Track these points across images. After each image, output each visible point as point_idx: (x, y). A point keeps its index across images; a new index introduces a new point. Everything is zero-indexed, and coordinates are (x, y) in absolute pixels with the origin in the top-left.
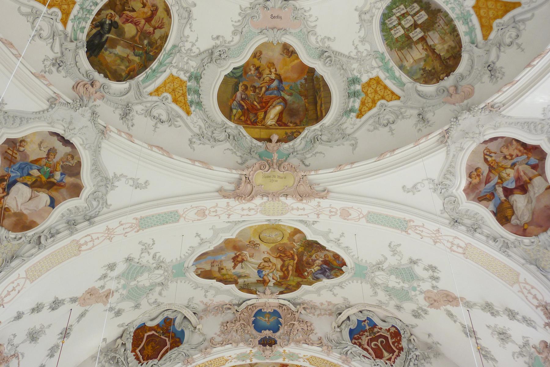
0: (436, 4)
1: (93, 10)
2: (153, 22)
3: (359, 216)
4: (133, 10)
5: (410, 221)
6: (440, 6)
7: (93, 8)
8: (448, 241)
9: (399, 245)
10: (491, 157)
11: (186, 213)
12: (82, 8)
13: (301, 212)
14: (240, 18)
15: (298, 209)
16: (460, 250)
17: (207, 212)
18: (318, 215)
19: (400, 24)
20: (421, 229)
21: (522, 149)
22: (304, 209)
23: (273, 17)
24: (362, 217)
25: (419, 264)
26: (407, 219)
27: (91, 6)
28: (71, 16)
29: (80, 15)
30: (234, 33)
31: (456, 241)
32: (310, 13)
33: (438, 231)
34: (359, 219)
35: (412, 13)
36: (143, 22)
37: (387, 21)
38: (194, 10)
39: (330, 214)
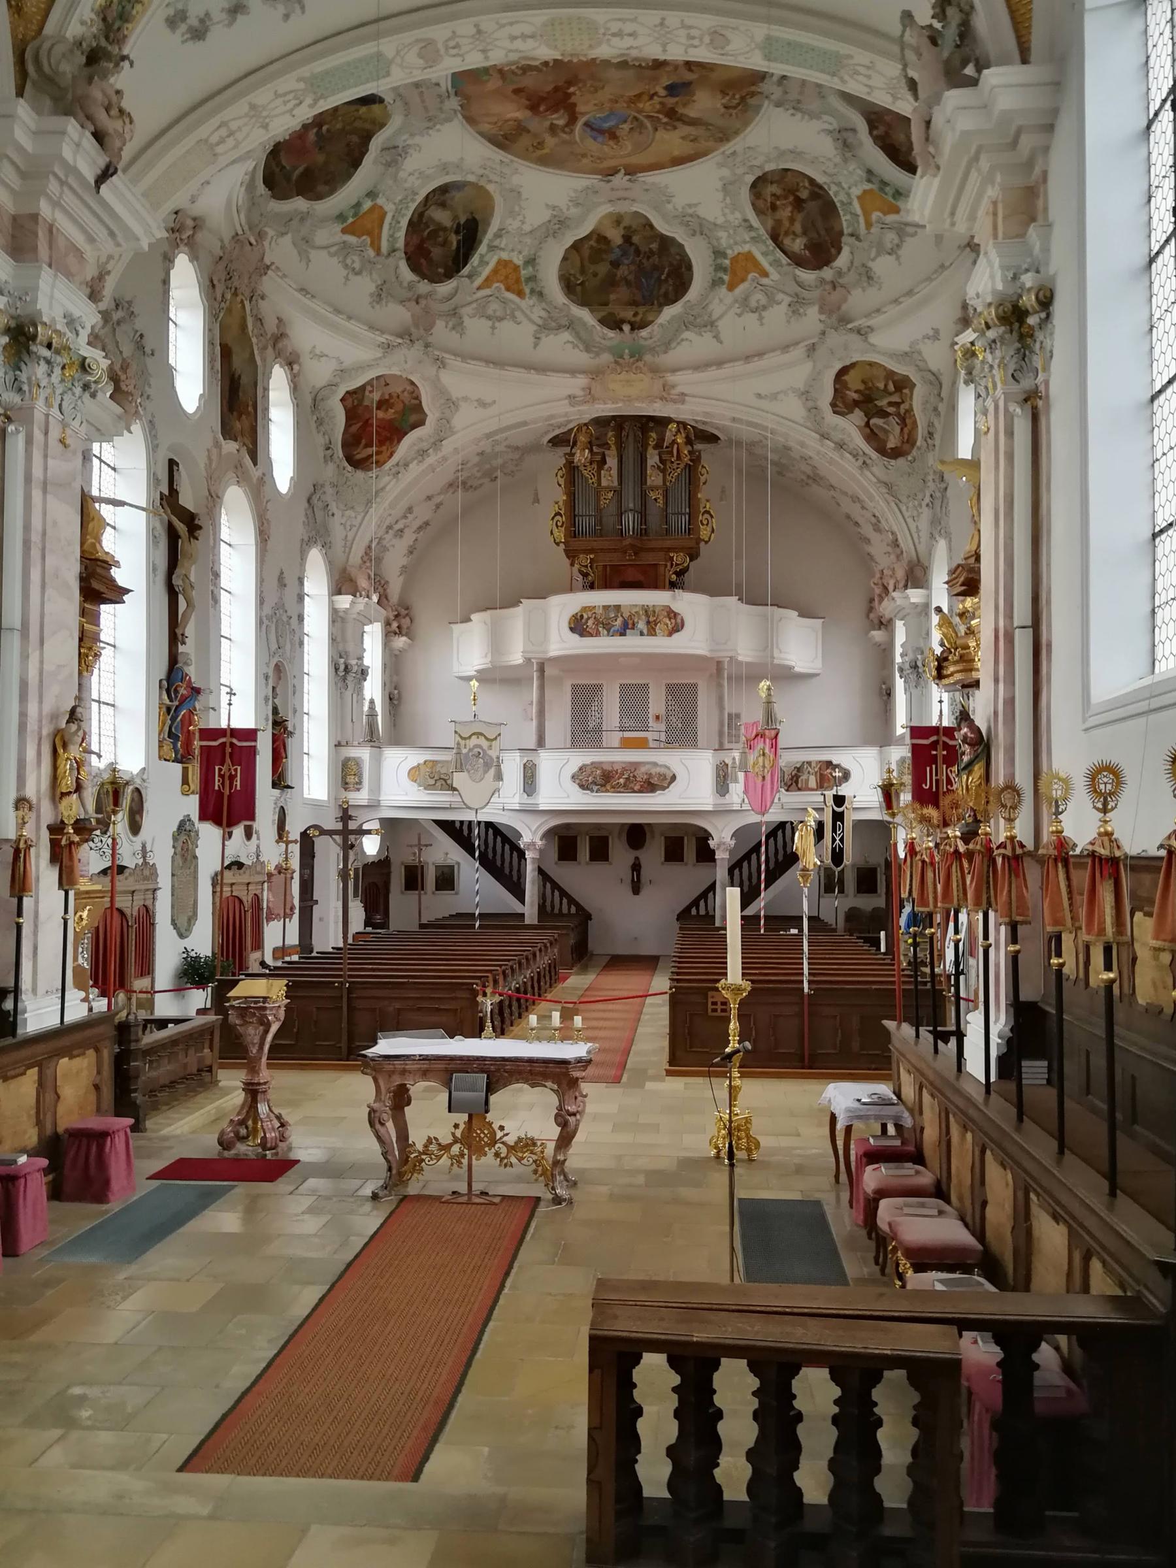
3: (402, 58)
5: (316, 101)
8: (240, 129)
9: (287, 17)
11: (748, 49)
13: (516, 30)
15: (524, 37)
16: (214, 139)
17: (707, 39)
18: (479, 32)
20: (290, 105)
22: (513, 38)
24: (394, 58)
25: (224, 16)
26: (321, 102)
31: (230, 142)
33: (265, 127)
34: (398, 52)
39: (457, 40)
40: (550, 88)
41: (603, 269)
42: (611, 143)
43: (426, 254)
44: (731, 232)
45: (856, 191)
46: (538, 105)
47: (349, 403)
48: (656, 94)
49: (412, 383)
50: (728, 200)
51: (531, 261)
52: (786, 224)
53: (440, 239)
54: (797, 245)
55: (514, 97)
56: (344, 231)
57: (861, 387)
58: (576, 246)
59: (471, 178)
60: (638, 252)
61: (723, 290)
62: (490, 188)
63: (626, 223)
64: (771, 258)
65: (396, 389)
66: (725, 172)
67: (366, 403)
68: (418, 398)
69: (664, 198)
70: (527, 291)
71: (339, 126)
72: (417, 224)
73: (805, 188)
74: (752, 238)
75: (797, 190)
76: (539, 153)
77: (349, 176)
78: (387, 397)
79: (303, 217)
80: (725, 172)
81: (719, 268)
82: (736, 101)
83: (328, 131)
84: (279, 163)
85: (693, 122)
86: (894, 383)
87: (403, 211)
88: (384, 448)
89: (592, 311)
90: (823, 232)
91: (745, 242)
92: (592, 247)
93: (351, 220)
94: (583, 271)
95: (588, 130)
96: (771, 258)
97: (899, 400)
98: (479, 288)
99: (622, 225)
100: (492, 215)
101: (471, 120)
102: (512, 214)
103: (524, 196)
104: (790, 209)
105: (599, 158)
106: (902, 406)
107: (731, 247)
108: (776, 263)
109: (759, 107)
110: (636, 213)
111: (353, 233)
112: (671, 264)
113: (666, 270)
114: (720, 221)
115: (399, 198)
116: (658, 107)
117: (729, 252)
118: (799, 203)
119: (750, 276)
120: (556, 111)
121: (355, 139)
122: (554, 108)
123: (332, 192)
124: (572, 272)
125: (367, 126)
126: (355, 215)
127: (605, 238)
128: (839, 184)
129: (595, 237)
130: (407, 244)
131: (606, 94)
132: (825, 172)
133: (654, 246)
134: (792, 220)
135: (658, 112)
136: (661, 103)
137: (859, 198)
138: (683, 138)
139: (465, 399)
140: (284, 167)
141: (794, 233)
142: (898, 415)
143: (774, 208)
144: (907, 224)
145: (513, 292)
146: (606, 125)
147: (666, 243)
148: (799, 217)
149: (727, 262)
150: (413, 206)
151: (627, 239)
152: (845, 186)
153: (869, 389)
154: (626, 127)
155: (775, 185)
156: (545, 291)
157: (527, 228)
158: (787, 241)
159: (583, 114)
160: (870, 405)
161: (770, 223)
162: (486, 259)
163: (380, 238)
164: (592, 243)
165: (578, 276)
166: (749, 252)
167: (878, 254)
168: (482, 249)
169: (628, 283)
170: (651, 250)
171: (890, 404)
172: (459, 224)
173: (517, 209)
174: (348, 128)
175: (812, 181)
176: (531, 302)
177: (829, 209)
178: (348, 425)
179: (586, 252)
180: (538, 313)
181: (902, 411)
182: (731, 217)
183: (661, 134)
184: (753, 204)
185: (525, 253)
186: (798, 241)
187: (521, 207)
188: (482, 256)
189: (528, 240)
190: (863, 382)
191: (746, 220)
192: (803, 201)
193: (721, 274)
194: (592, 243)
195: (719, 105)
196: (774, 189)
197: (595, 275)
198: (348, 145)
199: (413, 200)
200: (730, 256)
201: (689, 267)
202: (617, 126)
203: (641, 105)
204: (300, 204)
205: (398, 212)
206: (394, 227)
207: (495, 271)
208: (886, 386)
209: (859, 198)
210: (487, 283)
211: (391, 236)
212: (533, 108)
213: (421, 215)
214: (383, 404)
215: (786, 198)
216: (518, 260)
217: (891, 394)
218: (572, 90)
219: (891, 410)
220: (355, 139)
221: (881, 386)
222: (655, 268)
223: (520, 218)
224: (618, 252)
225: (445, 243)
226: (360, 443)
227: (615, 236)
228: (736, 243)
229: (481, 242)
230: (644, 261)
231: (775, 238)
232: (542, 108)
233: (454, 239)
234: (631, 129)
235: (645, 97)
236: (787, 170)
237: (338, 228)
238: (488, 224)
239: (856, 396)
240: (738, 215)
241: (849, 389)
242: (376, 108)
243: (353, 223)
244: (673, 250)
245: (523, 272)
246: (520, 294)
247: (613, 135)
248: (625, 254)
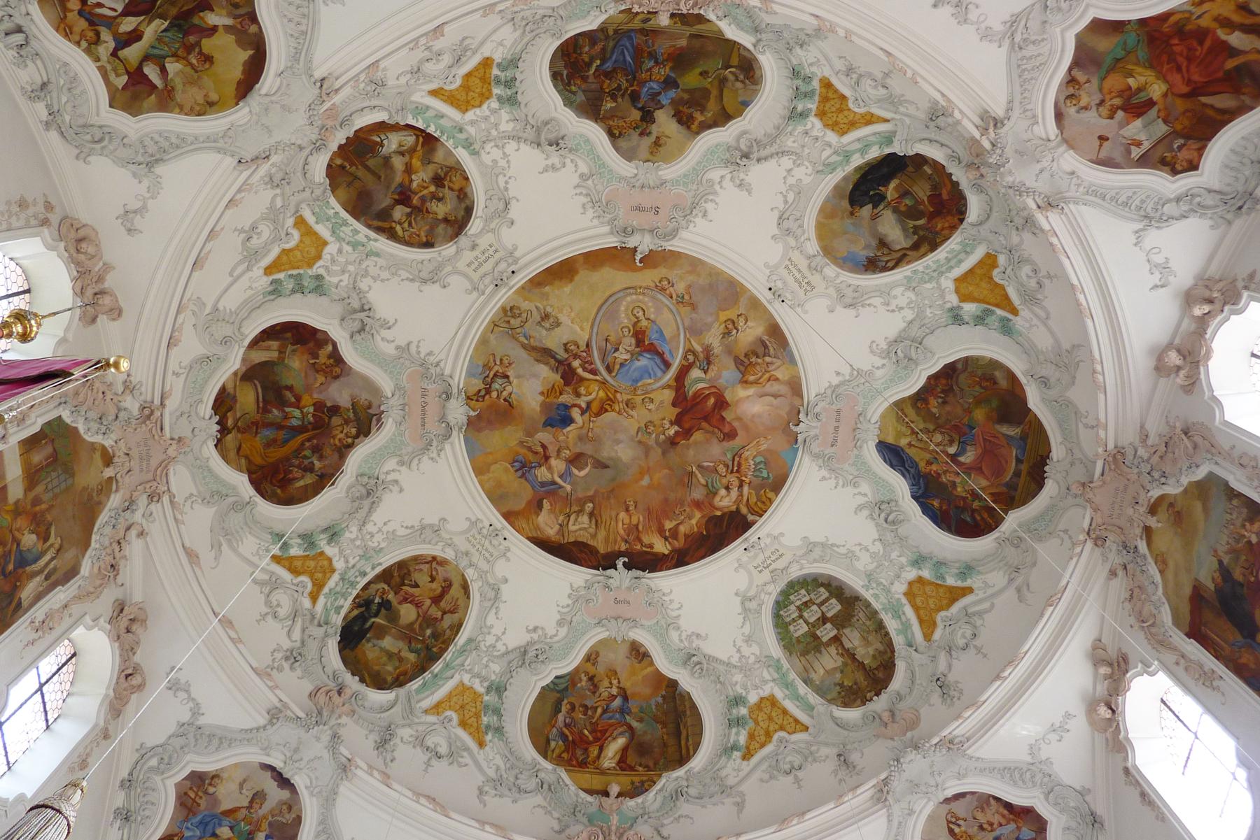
0: (851, 588)
1: (358, 583)
2: (443, 604)
4: (417, 586)
6: (857, 591)
7: (359, 579)
10: (959, 826)
12: (343, 579)
14: (570, 602)
19: (801, 617)
21: (1006, 812)
23: (617, 602)
27: (356, 577)
28: (326, 590)
29: (338, 589)
30: (560, 623)
32: (671, 597)
35: (818, 601)
36: (428, 602)
37: (781, 613)
38: (503, 587)
40: (697, 436)
41: (691, 79)
42: (644, 323)
43: (935, 198)
44: (494, 133)
45: (331, 249)
46: (715, 404)
47: (1184, 155)
48: (583, 412)
49: (1059, 116)
50: (501, 180)
51: (795, 115)
52: (416, 163)
53: (908, 202)
54: (392, 142)
55: (736, 424)
56: (1015, 312)
57: (207, 45)
58: (724, 117)
59: (831, 270)
60: (635, 97)
61: (498, 57)
62: (813, 247)
63: (647, 142)
64: (430, 114)
65: (1095, 121)
66: (508, 236)
67: (1161, 129)
68: (1071, 81)
69: (590, 182)
70: (816, 84)
71: (938, 437)
72: (927, 241)
73: (400, 223)
74: (461, 130)
75: (409, 215)
76: (731, 314)
77: (966, 360)
78: (1120, 114)
79: (1044, 382)
80: (508, 236)
81: (509, 83)
82: (496, 386)
83: (951, 442)
84: (1017, 474)
85: (544, 354)
86: (155, 87)
87: (934, 267)
88: (1205, 22)
89: (720, 32)
90: (361, 172)
91: (472, 123)
92: (703, 109)
93: (999, 312)
94: (723, 82)
95: (667, 356)
96: (430, 114)
97: (120, 53)
98: (887, 121)
99: (653, 138)
100: (826, 201)
101: (796, 388)
102: (798, 189)
103: (776, 214)
104: (415, 185)
105: (664, 290)
106: (112, 45)
107: (494, 111)
108: (420, 110)
109: (470, 374)
110: (629, 159)
111: (1006, 297)
112: (584, 79)
113: (592, 72)
114: (511, 146)
115: (929, 286)
116: (582, 390)
117: (494, 104)
118: (404, 197)
119: (458, 82)
120: (697, 394)
121: (934, 404)
122: (700, 398)
123: (995, 364)
124: (739, 85)
125: (911, 411)
126: (988, 313)
127: (680, 122)
128: (355, 245)
129: (694, 127)
130: (953, 228)
131: (639, 416)
132: (377, 255)
133: (609, 105)
134: (409, 170)
135: (582, 379)
136: (578, 395)
137: (325, 243)
138: (558, 324)
139: (986, 35)
140: (1019, 461)
141: (402, 154)
142: (110, 23)
143: (438, 180)
144: (249, 269)
145: (836, 91)
146: (644, 361)
147: (591, 109)
148: (398, 178)
149: (496, 91)
150: (919, 265)
151: (648, 117)
152: (349, 249)
153: (189, 49)
154: (622, 355)
155: (440, 217)
156: (787, 73)
157: (786, 162)
158: (410, 140)
159: (669, 386)
160: (173, 11)
161: (439, 156)
162: (858, 146)
163: (981, 263)
164: (699, 117)
165: (731, 77)
166: (465, 111)
167: (272, 207)
168: (857, 161)
169: (652, 56)
170: (614, 98)
171: (135, 36)
172: (875, 207)
173: (791, 197)
174: (931, 427)
175: (392, 235)
176: (814, 69)
177: (361, 207)
178: (1228, 116)
179: (712, 106)
180: (806, 57)
181: (106, 35)
182: (496, 154)
183: (583, 337)
184: (467, 179)
185: (800, 129)
186: (394, 147)
187: (786, 202)
188: (863, 151)
189: (790, 143)
190: (208, 59)
191: (475, 153)
192: (398, 202)
193: (502, 75)
194: (699, 117)
195: (515, 381)
196: (440, 210)
197: (704, 74)
198: (945, 403)
199: (915, 272)
200: (494, 99)
201: (555, 76)
202: (634, 356)
203: (602, 394)
204: (1034, 400)
205: (940, 272)
206: (949, 264)
207: (853, 125)
208: (163, 70)
209: (325, 243)
210: (870, 119)
211: (967, 253)
212: (722, 403)
213: (915, 247)
214: (1135, 106)
215: (423, 199)
216: (814, 123)
217: (146, 58)
218: (672, 432)
219: (128, 24)
220: (934, 404)
221: (173, 67)
222: (608, 75)
223: (791, 181)
224: (665, 100)
225: (905, 194)
226: (1237, 69)
227: (665, 122)
228: (486, 118)
229: (858, 168)
230: (625, 85)
231: (428, 141)
232: (712, 400)
233: (891, 191)
234: (617, 350)
235: (595, 407)
236: (428, 245)
237: (1019, 322)
238: (836, 187)
239: (212, 19)
240: (487, 159)
241: (228, 29)
242: (890, 440)
243: (997, 306)
244: (580, 97)
245: (812, 105)
246: (827, 85)
247: (639, 336)
248: (654, 96)
